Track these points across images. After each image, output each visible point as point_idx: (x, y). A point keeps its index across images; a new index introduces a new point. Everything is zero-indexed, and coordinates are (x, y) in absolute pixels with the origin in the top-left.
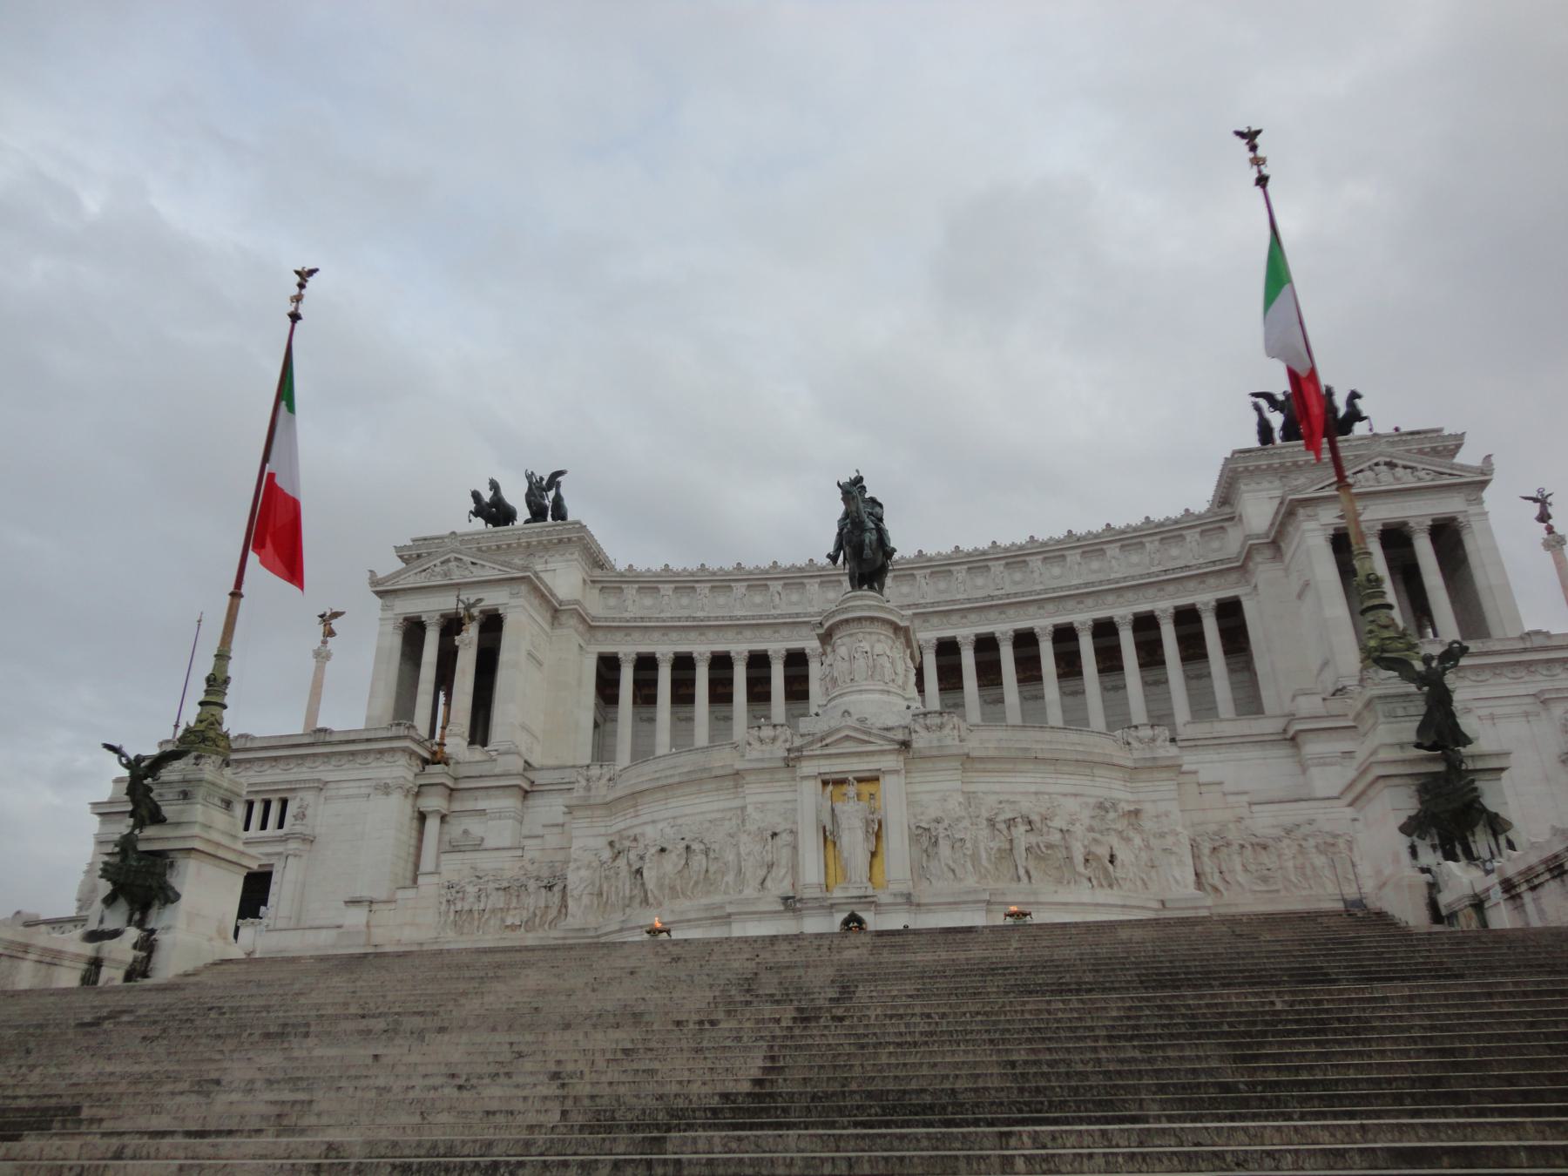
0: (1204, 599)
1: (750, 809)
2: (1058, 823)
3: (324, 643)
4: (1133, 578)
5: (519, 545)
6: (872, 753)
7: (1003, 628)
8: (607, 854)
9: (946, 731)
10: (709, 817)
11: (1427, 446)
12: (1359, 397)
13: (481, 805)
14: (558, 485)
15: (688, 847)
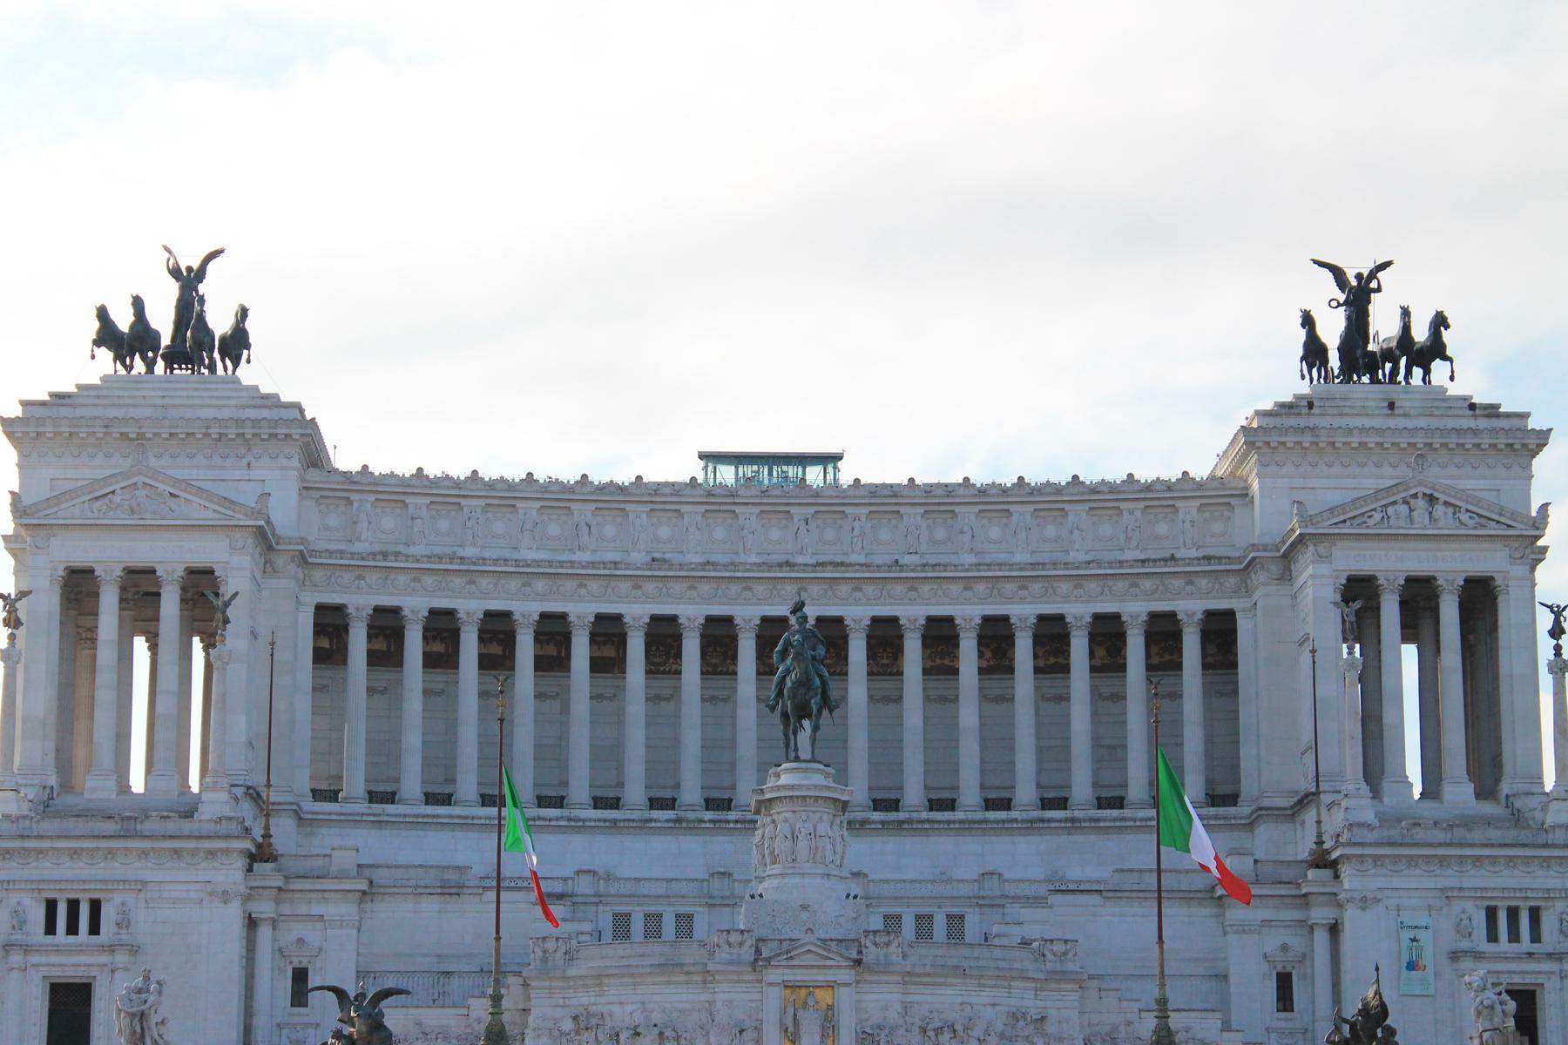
0: (1190, 607)
1: (719, 1005)
2: (977, 1032)
3: (12, 637)
4: (1099, 563)
5: (206, 435)
6: (831, 967)
7: (912, 613)
8: (568, 1025)
9: (892, 948)
10: (680, 1006)
11: (1502, 441)
12: (1447, 327)
13: (317, 909)
14: (244, 312)
15: (661, 1034)
